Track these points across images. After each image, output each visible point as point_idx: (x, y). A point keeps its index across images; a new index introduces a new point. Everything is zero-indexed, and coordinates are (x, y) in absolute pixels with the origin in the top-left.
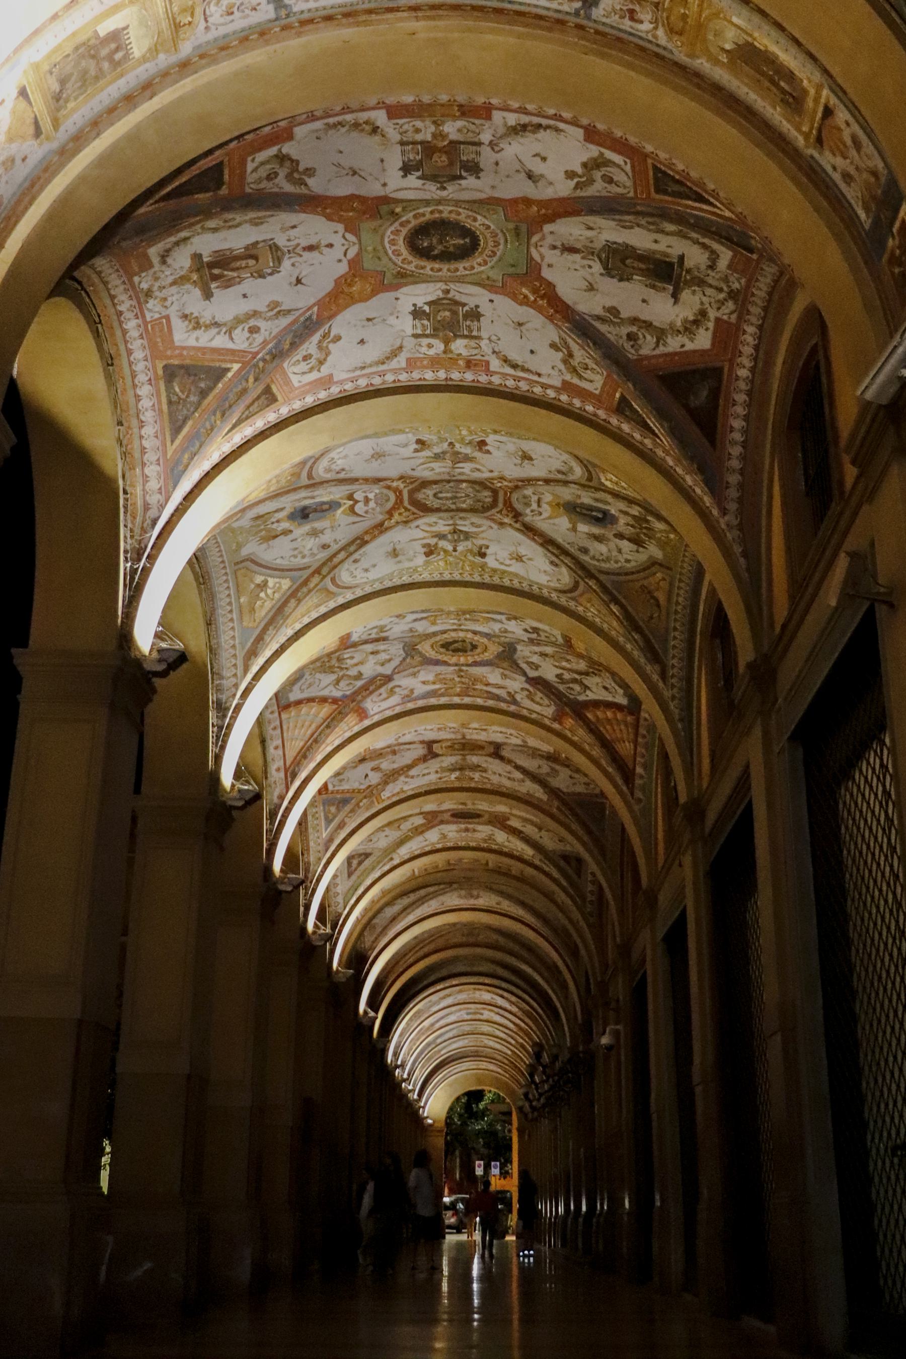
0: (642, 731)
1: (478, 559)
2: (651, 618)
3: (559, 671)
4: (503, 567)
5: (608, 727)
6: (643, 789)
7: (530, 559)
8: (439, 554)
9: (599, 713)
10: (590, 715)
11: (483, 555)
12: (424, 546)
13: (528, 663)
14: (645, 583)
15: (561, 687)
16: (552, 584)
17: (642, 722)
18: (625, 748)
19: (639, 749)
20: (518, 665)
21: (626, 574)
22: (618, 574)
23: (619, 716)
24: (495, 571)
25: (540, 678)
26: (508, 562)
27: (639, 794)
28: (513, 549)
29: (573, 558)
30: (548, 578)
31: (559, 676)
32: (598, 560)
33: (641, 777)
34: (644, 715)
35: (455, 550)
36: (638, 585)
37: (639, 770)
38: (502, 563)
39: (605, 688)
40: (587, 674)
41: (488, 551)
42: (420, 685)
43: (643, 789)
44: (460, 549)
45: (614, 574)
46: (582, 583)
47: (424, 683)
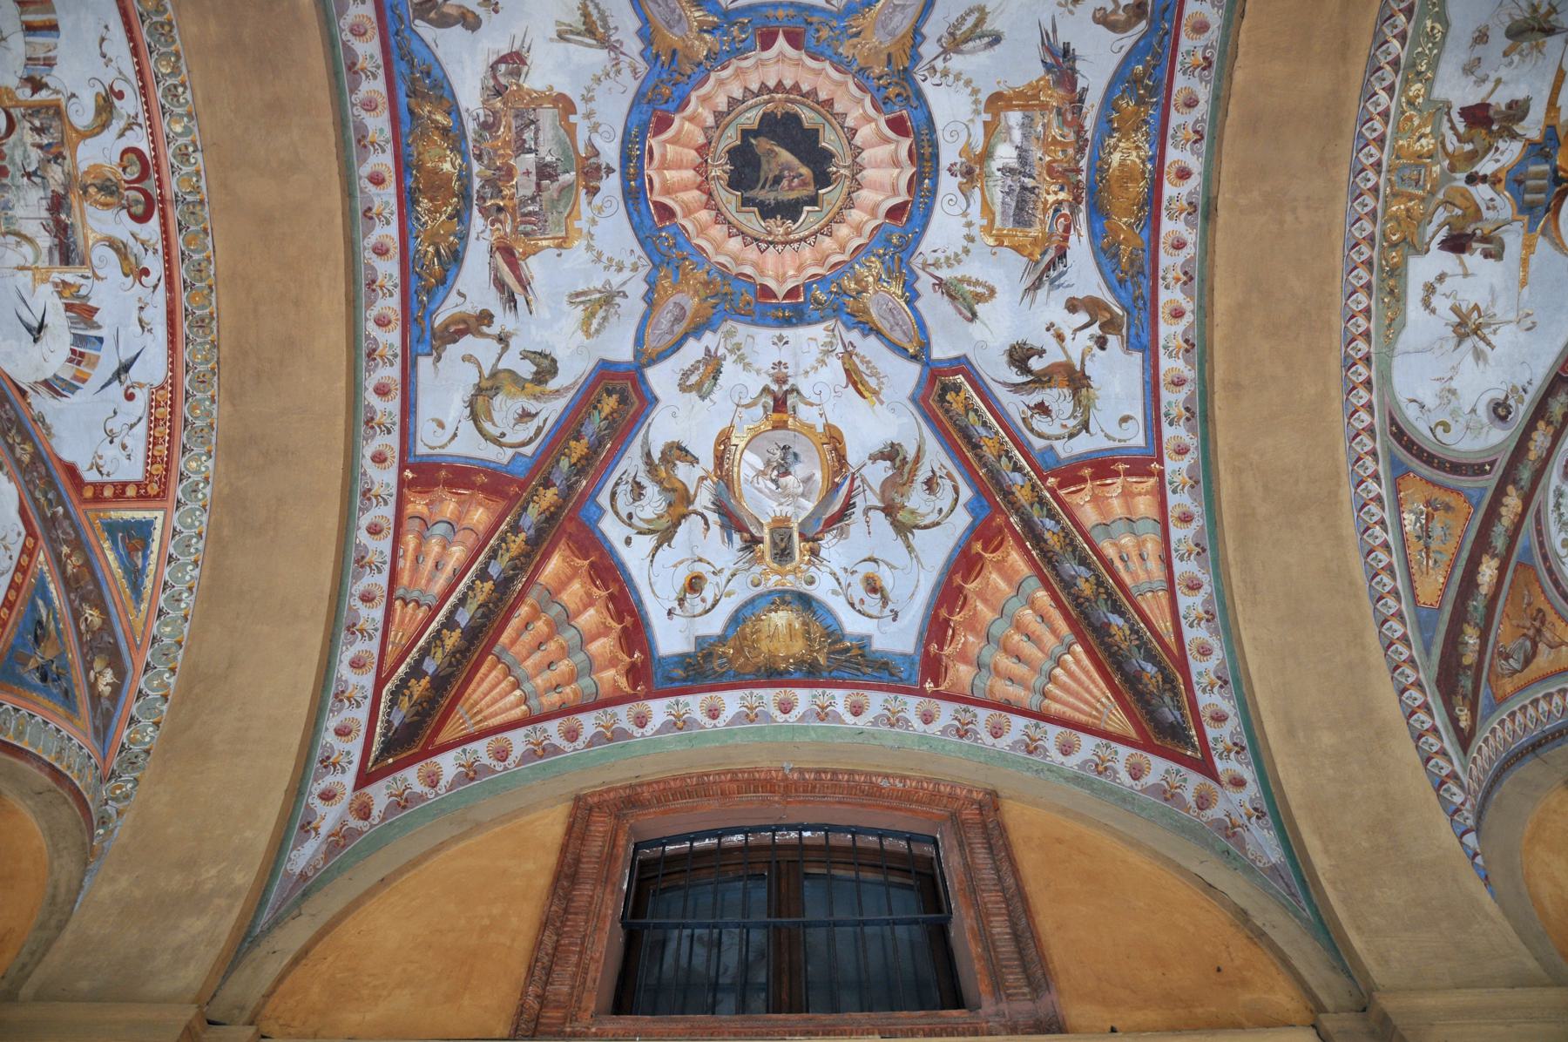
0: (589, 723)
1: (1436, 231)
2: (1507, 657)
3: (705, 452)
4: (1414, 293)
5: (540, 626)
6: (402, 802)
7: (1478, 355)
8: (1460, 139)
9: (576, 586)
10: (555, 565)
11: (1457, 243)
12: (1518, 110)
13: (712, 366)
14: (1551, 616)
15: (631, 463)
16: (1411, 412)
17: (623, 715)
18: (491, 695)
19: (518, 741)
20: (696, 331)
21: (1550, 571)
22: (1545, 558)
23: (602, 646)
24: (1397, 272)
25: (649, 401)
26: (1441, 303)
27: (380, 794)
28: (1501, 310)
29: (1551, 451)
30: (1431, 402)
31: (678, 452)
32: (1558, 505)
33: (432, 780)
34: (659, 710)
35: (1472, 179)
36: (1541, 602)
37: (448, 764)
38: (1430, 289)
39: (694, 584)
40: (732, 521)
41: (1474, 260)
42: (493, 40)
43: (402, 802)
44: (1482, 192)
45: (1542, 545)
46: (1490, 481)
47: (515, 60)
